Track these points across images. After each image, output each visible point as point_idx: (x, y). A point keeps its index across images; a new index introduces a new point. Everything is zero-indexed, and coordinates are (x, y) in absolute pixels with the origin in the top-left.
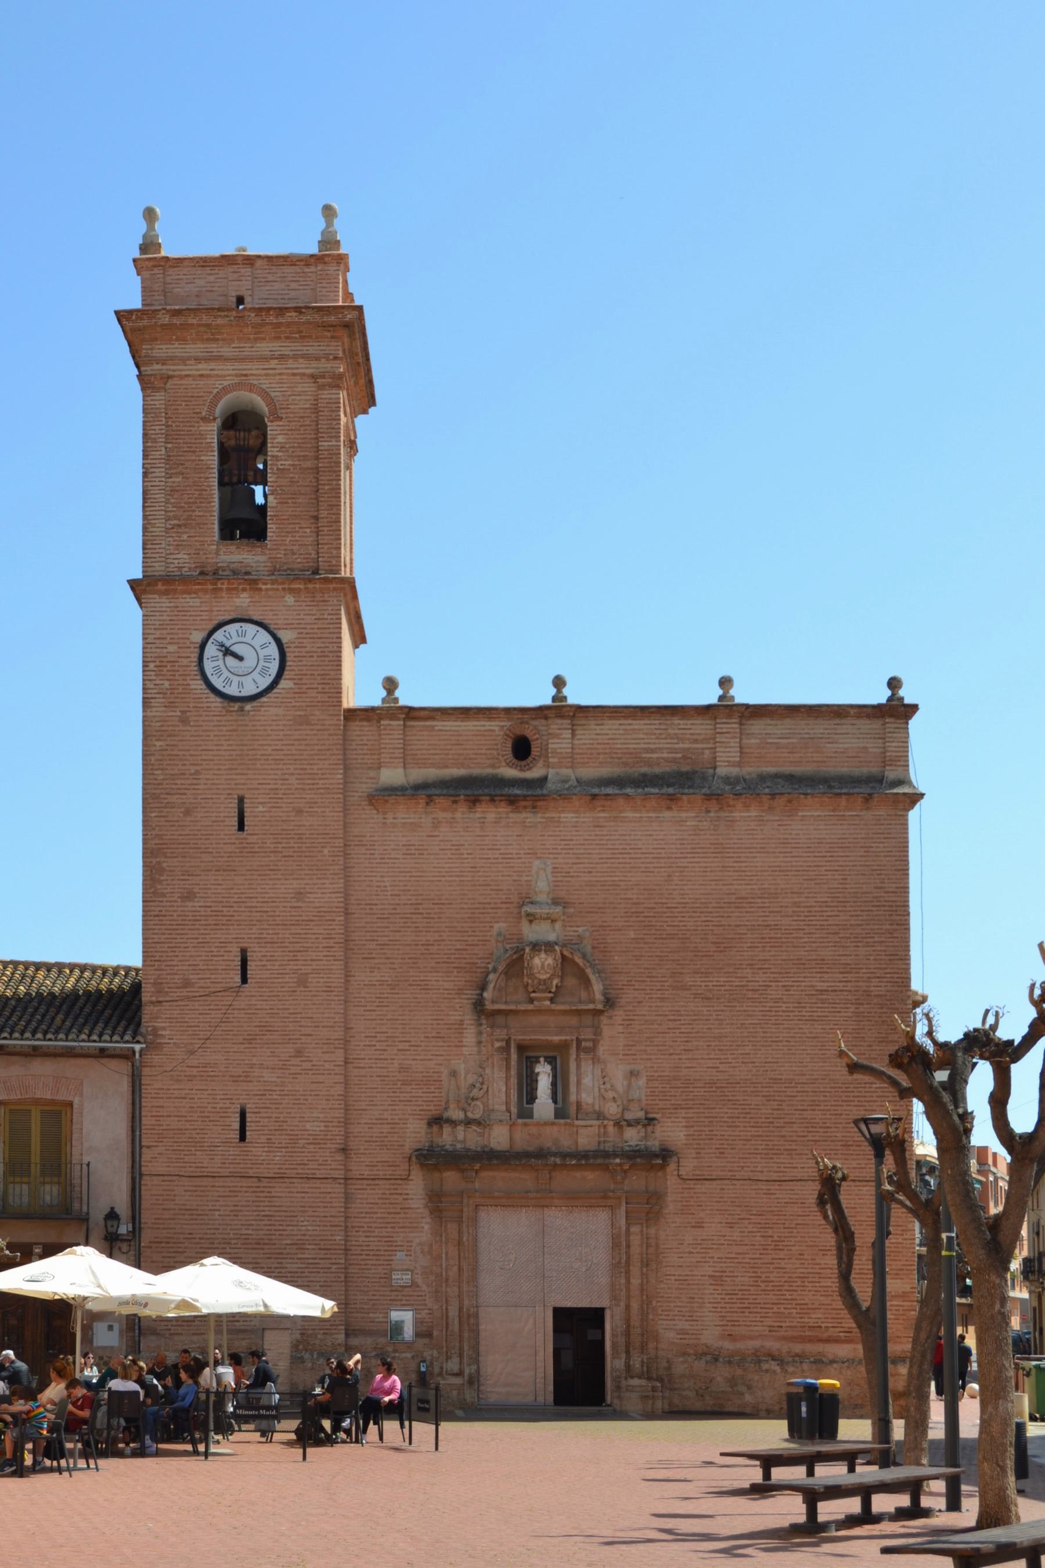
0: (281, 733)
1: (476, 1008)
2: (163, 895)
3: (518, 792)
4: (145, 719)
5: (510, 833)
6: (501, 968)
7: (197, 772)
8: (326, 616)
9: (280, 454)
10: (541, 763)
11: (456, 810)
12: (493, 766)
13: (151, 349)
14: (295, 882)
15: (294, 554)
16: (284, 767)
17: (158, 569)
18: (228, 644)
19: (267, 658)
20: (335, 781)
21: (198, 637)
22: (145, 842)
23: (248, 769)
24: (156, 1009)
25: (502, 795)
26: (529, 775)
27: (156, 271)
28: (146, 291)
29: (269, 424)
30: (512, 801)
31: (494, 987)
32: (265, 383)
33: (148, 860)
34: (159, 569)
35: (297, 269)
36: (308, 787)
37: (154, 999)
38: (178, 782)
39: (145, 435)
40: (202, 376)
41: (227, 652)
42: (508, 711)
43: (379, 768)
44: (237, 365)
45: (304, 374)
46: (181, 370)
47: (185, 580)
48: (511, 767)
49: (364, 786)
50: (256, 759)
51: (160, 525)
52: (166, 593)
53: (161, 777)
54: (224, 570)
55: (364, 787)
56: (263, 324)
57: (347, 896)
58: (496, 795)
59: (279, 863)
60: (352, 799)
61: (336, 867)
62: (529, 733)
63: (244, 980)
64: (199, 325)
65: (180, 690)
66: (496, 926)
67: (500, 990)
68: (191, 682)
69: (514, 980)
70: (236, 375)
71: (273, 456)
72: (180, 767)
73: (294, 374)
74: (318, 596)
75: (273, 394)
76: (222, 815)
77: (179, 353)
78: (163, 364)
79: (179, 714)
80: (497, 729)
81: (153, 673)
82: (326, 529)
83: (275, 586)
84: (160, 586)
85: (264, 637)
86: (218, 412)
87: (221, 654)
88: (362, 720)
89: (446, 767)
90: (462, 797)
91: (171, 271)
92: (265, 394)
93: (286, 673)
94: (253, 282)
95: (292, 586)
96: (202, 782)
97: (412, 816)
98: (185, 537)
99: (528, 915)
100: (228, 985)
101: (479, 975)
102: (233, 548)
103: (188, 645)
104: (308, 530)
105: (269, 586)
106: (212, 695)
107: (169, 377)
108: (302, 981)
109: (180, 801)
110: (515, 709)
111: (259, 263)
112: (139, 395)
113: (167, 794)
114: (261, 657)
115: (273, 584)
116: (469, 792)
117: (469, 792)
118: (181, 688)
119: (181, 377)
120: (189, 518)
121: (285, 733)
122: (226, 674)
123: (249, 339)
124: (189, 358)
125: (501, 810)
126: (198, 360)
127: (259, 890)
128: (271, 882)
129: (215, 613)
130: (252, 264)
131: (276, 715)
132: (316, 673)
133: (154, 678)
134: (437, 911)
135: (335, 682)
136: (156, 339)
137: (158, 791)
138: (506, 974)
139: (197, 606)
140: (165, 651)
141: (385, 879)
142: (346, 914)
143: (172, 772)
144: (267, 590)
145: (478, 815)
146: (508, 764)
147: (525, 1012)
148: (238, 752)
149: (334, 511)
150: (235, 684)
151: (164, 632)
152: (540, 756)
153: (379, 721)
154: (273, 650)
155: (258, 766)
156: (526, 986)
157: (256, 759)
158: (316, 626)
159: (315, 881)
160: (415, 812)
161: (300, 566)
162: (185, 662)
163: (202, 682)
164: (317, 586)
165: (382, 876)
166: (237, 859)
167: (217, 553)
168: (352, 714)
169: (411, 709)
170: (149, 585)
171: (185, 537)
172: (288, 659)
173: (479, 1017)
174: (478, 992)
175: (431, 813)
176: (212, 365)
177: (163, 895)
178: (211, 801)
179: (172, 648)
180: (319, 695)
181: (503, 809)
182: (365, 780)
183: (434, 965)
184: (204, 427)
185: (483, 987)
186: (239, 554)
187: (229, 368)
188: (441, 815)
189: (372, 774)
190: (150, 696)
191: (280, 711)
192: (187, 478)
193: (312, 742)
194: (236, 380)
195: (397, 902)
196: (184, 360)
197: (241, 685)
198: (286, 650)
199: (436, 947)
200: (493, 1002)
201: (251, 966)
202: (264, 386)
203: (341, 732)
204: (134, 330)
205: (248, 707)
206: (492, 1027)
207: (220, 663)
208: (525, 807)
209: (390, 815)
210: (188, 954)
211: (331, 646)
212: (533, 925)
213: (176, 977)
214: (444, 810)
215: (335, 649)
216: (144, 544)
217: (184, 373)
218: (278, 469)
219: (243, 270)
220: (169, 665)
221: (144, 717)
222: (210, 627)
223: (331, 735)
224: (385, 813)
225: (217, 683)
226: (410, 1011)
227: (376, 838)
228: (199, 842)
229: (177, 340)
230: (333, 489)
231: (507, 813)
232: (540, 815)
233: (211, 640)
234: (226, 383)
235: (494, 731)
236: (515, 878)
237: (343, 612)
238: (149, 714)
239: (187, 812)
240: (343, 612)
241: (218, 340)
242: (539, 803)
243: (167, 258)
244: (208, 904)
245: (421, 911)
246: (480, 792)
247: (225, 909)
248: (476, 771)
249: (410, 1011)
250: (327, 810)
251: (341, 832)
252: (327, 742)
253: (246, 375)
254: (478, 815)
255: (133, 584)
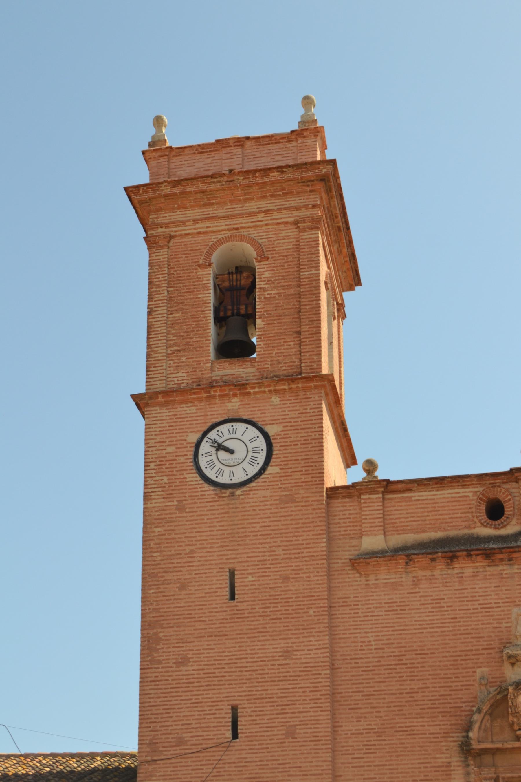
0: (269, 511)
1: (462, 749)
2: (160, 662)
3: (494, 546)
4: (146, 510)
5: (488, 585)
6: (485, 709)
7: (192, 552)
8: (308, 411)
9: (266, 286)
10: (514, 522)
11: (435, 567)
12: (468, 527)
13: (157, 218)
14: (283, 641)
15: (279, 363)
16: (272, 540)
17: (159, 386)
18: (220, 441)
19: (256, 450)
20: (319, 549)
21: (194, 438)
22: (143, 616)
23: (239, 545)
24: (150, 767)
25: (478, 550)
26: (503, 532)
27: (162, 160)
28: (152, 174)
29: (256, 264)
30: (488, 555)
31: (480, 727)
32: (253, 233)
33: (145, 632)
34: (160, 386)
35: (281, 145)
36: (293, 556)
37: (149, 758)
38: (175, 561)
39: (150, 283)
40: (199, 233)
41: (220, 447)
42: (480, 477)
43: (361, 537)
44: (229, 222)
45: (287, 223)
46: (182, 231)
47: (181, 391)
48: (486, 526)
49: (347, 553)
50: (246, 536)
51: (161, 352)
52: (166, 404)
53: (159, 558)
54: (217, 383)
55: (345, 553)
56: (249, 186)
57: (332, 652)
58: (472, 550)
59: (267, 626)
60: (336, 565)
61: (322, 626)
62: (501, 496)
63: (235, 735)
64: (196, 193)
65: (178, 483)
66: (479, 671)
67: (485, 730)
68: (187, 476)
69: (499, 720)
70: (229, 230)
71: (260, 288)
72: (177, 548)
73: (279, 224)
74: (301, 394)
75: (260, 241)
76: (214, 586)
77: (180, 218)
78: (166, 227)
79: (176, 503)
80: (470, 494)
81: (153, 471)
82: (307, 340)
83: (262, 389)
84: (160, 399)
85: (253, 432)
86: (214, 258)
87: (213, 450)
88: (344, 497)
89: (424, 531)
90: (440, 554)
91: (175, 160)
92: (253, 242)
93: (272, 460)
94: (243, 160)
95: (277, 388)
96: (196, 559)
97: (393, 576)
98: (184, 359)
99: (510, 657)
100: (218, 741)
101: (464, 718)
102: (226, 365)
103: (185, 445)
104: (292, 343)
105: (257, 390)
106: (206, 485)
107: (171, 237)
108: (291, 733)
109: (176, 578)
110: (486, 475)
111: (248, 144)
112: (147, 253)
113: (164, 572)
114: (250, 449)
115: (260, 387)
116: (446, 549)
117: (446, 549)
118: (178, 481)
119: (181, 236)
120: (188, 344)
121: (273, 511)
122: (218, 465)
123: (240, 201)
124: (189, 221)
125: (478, 564)
126: (196, 221)
127: (249, 652)
128: (259, 643)
129: (209, 417)
130: (242, 146)
131: (265, 497)
132: (300, 458)
133: (154, 475)
134: (420, 660)
135: (317, 464)
136: (160, 209)
137: (155, 571)
138: (491, 715)
139: (193, 414)
140: (164, 452)
141: (370, 635)
142: (333, 669)
143: (169, 553)
144: (255, 393)
145: (456, 571)
146: (482, 524)
147: (513, 750)
148: (230, 531)
149: (315, 325)
150: (226, 474)
151: (164, 436)
152: (513, 515)
153: (359, 497)
154: (261, 443)
155: (248, 542)
156: (512, 725)
157: (246, 536)
158: (300, 419)
159: (301, 640)
160: (396, 573)
161: (285, 372)
162: (182, 459)
163: (197, 475)
164: (300, 385)
165: (366, 633)
166: (228, 625)
167: (212, 370)
168: (334, 492)
169: (388, 482)
170: (150, 398)
171: (184, 359)
172: (274, 448)
173: (466, 758)
174: (464, 734)
175: (411, 572)
176: (208, 224)
177: (160, 662)
178: (204, 576)
179: (170, 449)
180: (303, 477)
181: (480, 563)
182: (348, 548)
183: (420, 711)
184: (201, 272)
185: (468, 728)
186: (231, 369)
187: (222, 224)
188: (421, 573)
189: (354, 542)
190: (150, 490)
191: (268, 493)
192: (185, 313)
193: (298, 517)
194: (229, 233)
195: (381, 655)
196: (184, 223)
197: (232, 474)
198: (273, 441)
199: (420, 694)
200: (479, 742)
201: (241, 721)
202: (253, 236)
203: (323, 506)
204: (141, 202)
205: (238, 492)
206: (479, 767)
207: (214, 457)
208: (501, 560)
209: (372, 577)
210: (182, 714)
211: (313, 434)
212: (516, 667)
213: (171, 736)
214: (423, 569)
215: (317, 436)
216: (148, 367)
217: (184, 232)
218: (265, 298)
219: (234, 151)
220: (168, 463)
221: (144, 508)
222: (205, 428)
223: (314, 509)
224: (367, 575)
225: (211, 474)
226: (398, 756)
227: (360, 599)
228: (193, 612)
229: (179, 208)
230: (313, 308)
231: (484, 567)
232: (516, 567)
233: (206, 439)
234: (220, 237)
235: (469, 496)
236: (495, 625)
237: (324, 406)
238: (149, 505)
239: (182, 587)
240: (324, 406)
241: (213, 204)
242: (515, 555)
243: (171, 147)
244: (201, 667)
245: (404, 662)
246: (457, 549)
247: (216, 671)
248: (452, 533)
249: (398, 756)
250: (312, 575)
251: (326, 593)
252: (311, 516)
253: (237, 229)
254: (456, 571)
255: (136, 398)
